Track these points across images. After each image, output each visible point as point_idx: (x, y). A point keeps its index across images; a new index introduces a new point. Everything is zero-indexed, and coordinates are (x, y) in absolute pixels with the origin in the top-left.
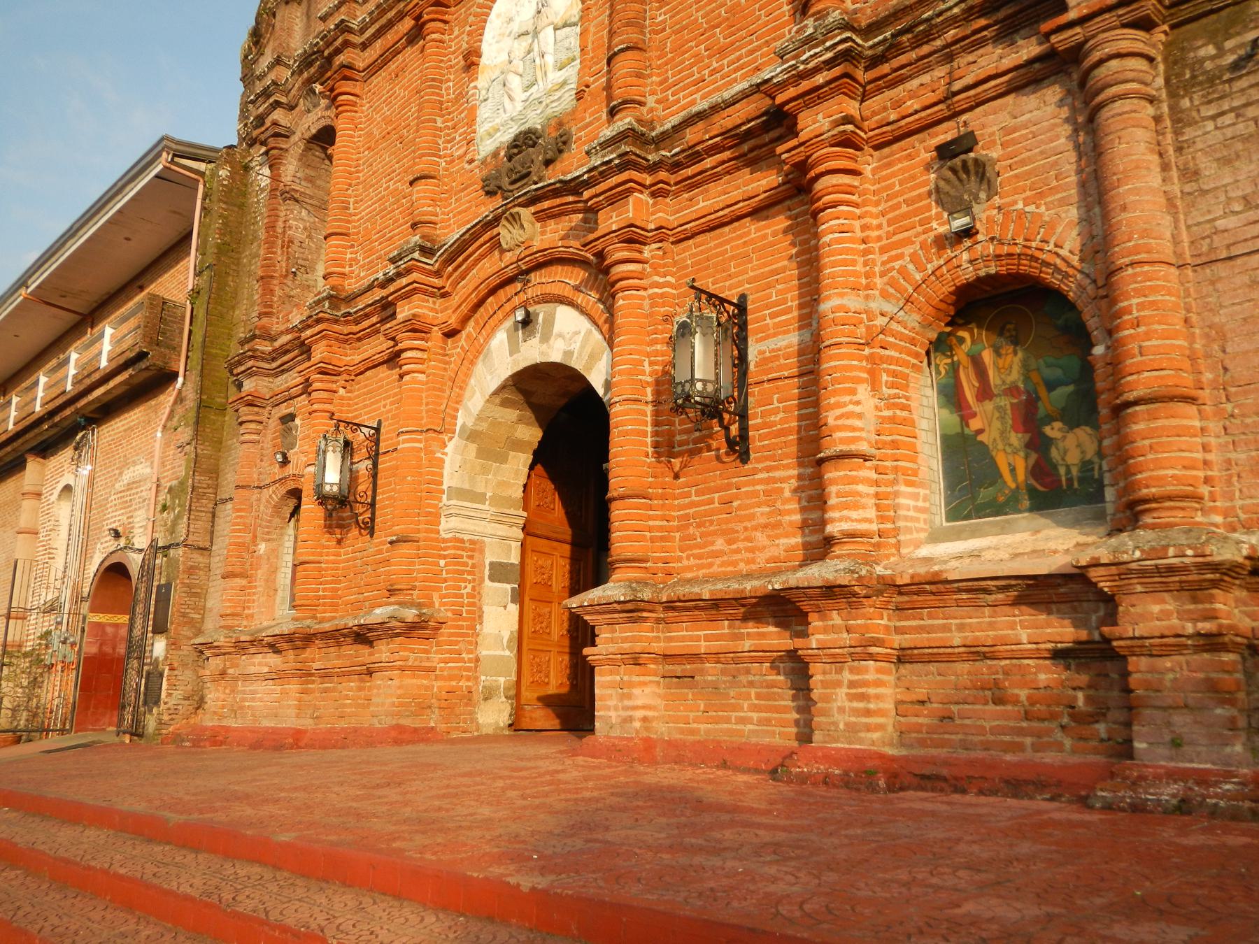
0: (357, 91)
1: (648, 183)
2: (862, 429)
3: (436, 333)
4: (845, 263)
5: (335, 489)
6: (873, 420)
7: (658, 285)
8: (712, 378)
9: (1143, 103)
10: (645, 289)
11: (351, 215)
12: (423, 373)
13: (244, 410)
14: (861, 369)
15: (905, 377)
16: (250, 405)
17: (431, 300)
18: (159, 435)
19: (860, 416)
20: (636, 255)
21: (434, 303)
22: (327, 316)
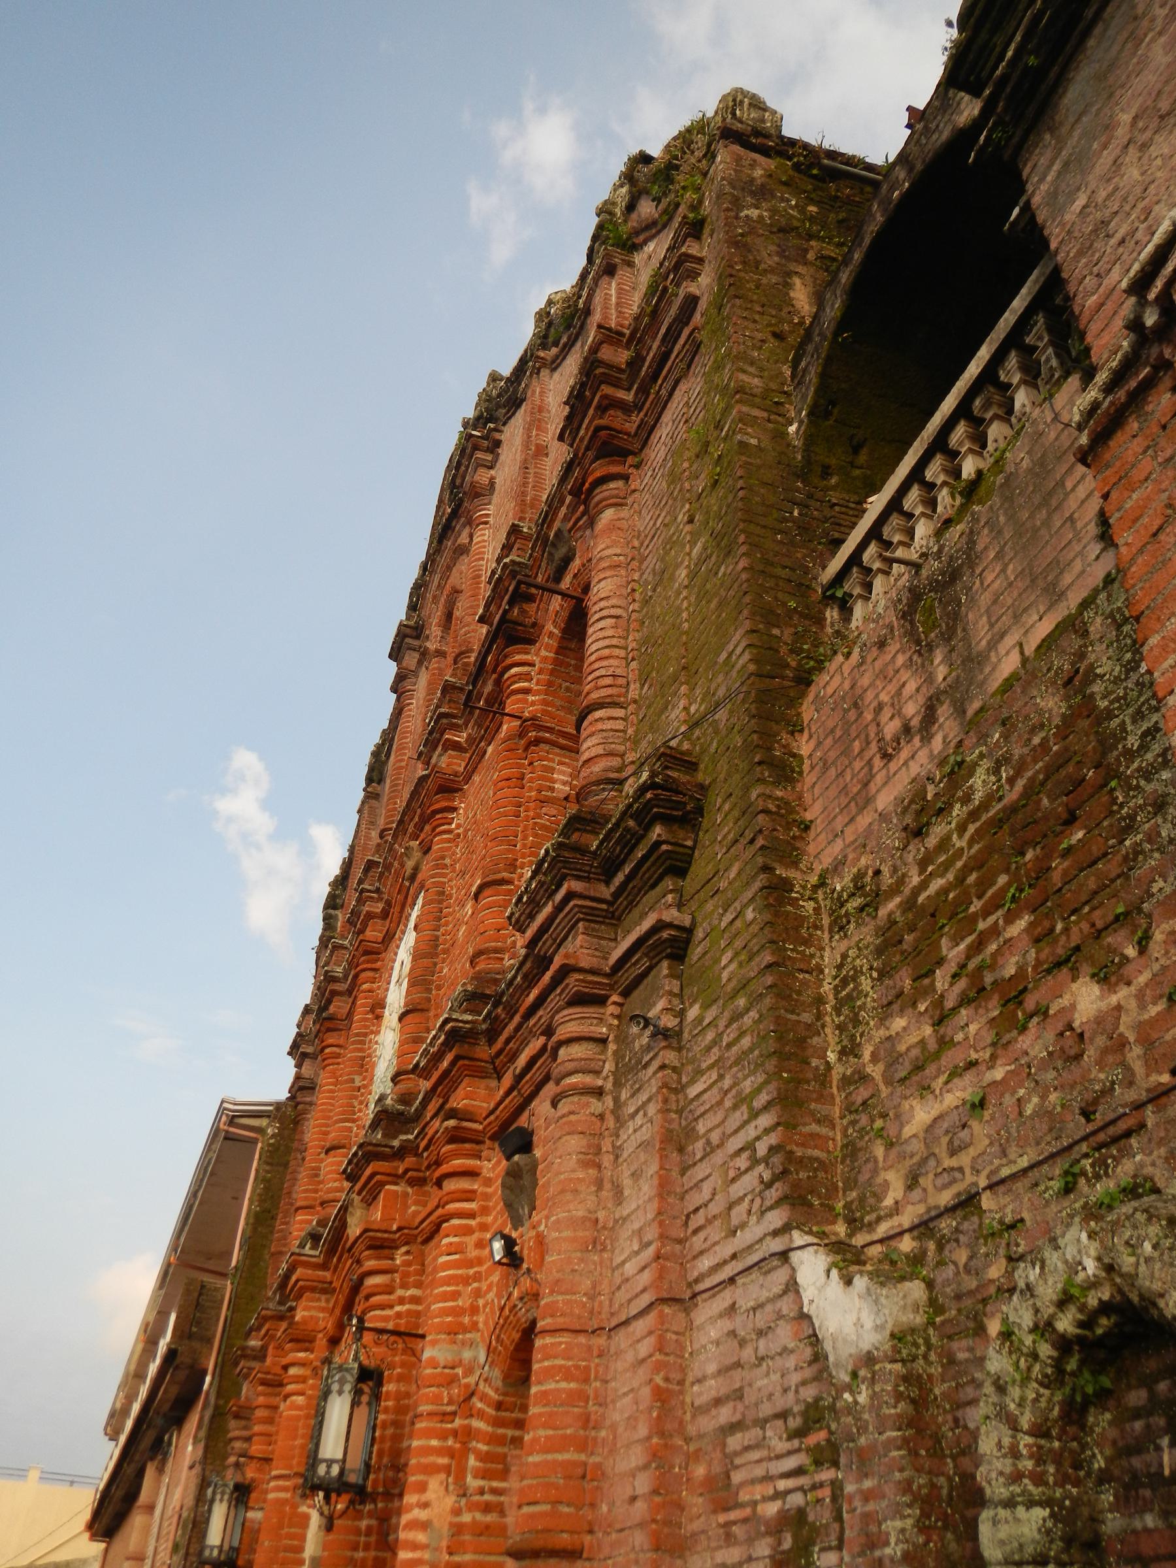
0: (341, 1041)
1: (401, 1171)
2: (423, 1547)
3: (321, 1341)
4: (445, 1297)
5: (215, 1553)
6: (445, 1531)
7: (401, 1301)
8: (340, 1456)
9: (584, 1099)
10: (391, 1307)
11: (322, 1182)
12: (302, 1394)
13: (233, 1424)
14: (439, 1451)
15: (502, 1458)
16: (237, 1416)
17: (323, 1297)
18: (190, 1448)
19: (424, 1526)
20: (385, 1264)
21: (327, 1301)
22: (269, 1313)
